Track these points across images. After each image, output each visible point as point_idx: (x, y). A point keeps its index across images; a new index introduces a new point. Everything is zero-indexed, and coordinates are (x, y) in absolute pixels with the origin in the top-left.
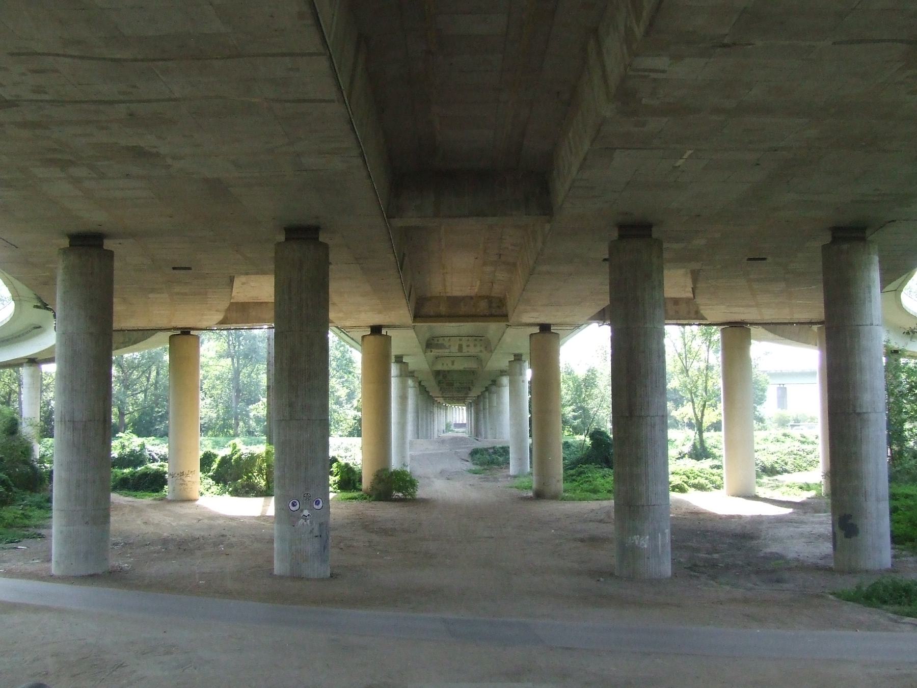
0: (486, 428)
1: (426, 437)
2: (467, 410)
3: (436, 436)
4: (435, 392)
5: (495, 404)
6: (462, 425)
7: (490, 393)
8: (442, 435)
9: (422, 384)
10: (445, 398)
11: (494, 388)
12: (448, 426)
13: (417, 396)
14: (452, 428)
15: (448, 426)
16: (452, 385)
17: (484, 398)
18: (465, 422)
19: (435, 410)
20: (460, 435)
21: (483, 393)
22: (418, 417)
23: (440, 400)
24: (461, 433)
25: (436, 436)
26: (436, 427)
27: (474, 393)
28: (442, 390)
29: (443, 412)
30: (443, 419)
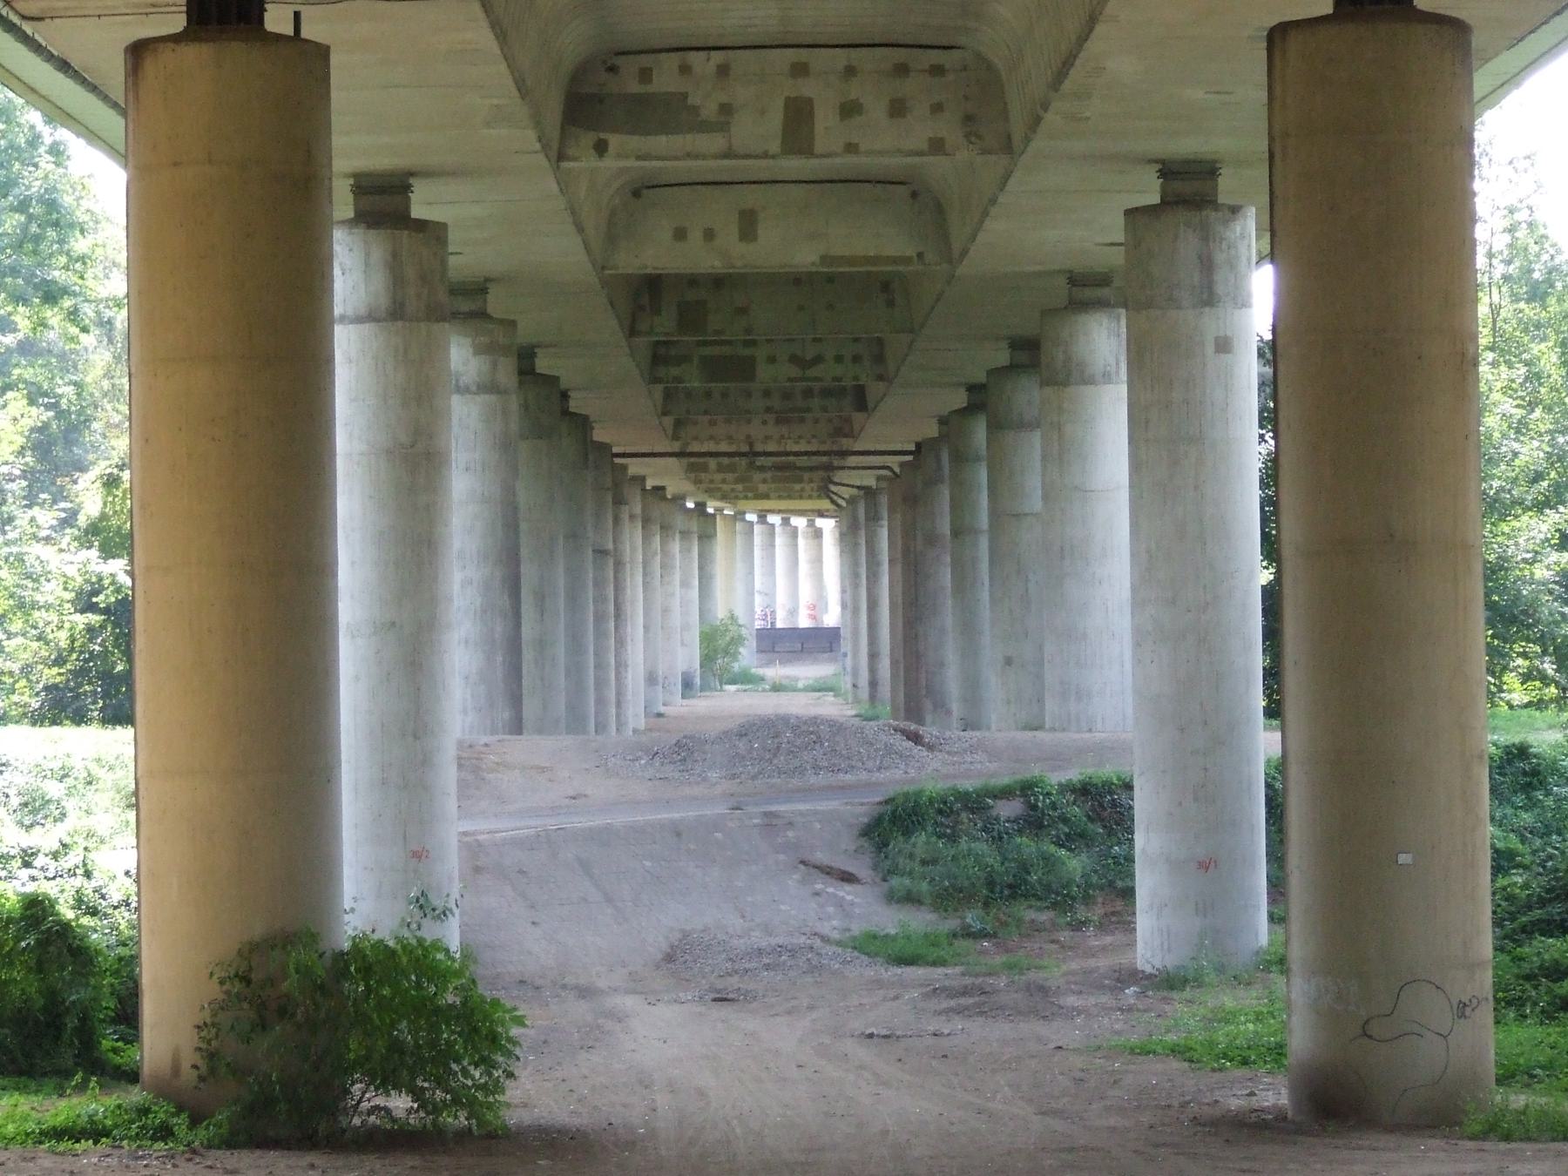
0: (970, 651)
1: (575, 723)
2: (848, 537)
3: (636, 717)
4: (625, 418)
5: (1036, 503)
6: (817, 642)
7: (997, 426)
8: (677, 705)
9: (543, 365)
10: (694, 461)
11: (1026, 395)
12: (716, 647)
13: (505, 446)
14: (747, 657)
15: (716, 647)
16: (741, 369)
17: (961, 458)
18: (832, 617)
19: (633, 538)
20: (797, 705)
21: (952, 424)
22: (513, 585)
23: (668, 475)
24: (806, 691)
25: (636, 717)
26: (636, 655)
27: (893, 428)
28: (677, 409)
29: (681, 555)
30: (681, 598)
